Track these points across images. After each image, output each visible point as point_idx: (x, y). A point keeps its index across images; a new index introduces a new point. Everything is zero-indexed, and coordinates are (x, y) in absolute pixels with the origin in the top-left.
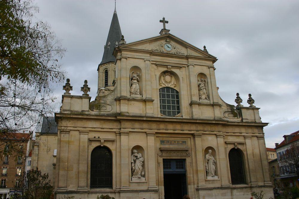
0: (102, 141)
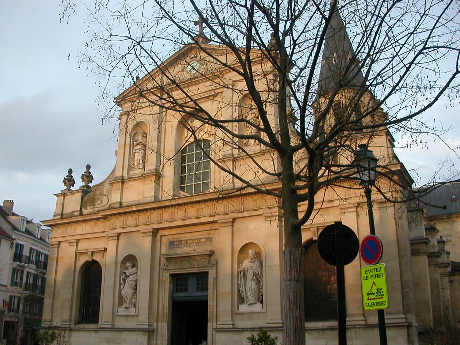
0: (90, 253)
